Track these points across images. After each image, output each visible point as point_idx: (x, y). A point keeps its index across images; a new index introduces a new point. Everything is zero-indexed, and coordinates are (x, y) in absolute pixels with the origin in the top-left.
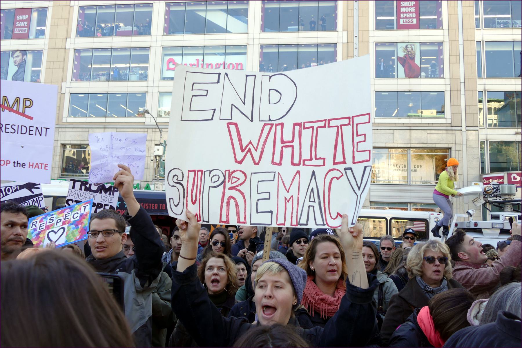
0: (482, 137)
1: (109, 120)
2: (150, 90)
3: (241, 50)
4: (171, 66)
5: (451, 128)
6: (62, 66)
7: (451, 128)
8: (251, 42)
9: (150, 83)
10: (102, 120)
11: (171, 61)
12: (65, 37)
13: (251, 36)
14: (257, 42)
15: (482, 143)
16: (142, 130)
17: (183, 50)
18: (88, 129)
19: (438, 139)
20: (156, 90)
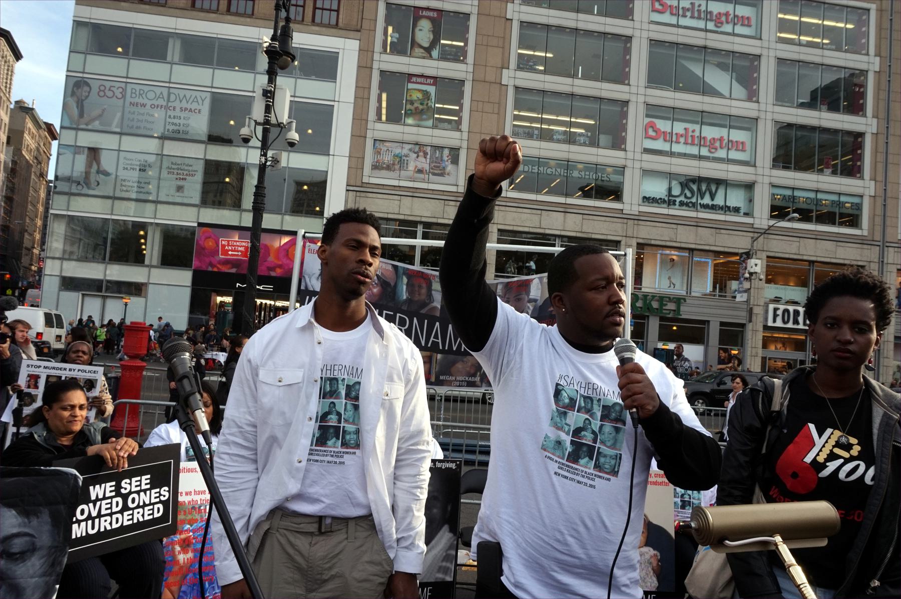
1: (570, 201)
2: (629, 164)
3: (750, 124)
4: (651, 133)
6: (496, 111)
8: (762, 115)
9: (630, 155)
10: (561, 200)
11: (652, 126)
12: (500, 66)
14: (769, 116)
16: (620, 220)
17: (674, 113)
18: (539, 212)
20: (637, 165)
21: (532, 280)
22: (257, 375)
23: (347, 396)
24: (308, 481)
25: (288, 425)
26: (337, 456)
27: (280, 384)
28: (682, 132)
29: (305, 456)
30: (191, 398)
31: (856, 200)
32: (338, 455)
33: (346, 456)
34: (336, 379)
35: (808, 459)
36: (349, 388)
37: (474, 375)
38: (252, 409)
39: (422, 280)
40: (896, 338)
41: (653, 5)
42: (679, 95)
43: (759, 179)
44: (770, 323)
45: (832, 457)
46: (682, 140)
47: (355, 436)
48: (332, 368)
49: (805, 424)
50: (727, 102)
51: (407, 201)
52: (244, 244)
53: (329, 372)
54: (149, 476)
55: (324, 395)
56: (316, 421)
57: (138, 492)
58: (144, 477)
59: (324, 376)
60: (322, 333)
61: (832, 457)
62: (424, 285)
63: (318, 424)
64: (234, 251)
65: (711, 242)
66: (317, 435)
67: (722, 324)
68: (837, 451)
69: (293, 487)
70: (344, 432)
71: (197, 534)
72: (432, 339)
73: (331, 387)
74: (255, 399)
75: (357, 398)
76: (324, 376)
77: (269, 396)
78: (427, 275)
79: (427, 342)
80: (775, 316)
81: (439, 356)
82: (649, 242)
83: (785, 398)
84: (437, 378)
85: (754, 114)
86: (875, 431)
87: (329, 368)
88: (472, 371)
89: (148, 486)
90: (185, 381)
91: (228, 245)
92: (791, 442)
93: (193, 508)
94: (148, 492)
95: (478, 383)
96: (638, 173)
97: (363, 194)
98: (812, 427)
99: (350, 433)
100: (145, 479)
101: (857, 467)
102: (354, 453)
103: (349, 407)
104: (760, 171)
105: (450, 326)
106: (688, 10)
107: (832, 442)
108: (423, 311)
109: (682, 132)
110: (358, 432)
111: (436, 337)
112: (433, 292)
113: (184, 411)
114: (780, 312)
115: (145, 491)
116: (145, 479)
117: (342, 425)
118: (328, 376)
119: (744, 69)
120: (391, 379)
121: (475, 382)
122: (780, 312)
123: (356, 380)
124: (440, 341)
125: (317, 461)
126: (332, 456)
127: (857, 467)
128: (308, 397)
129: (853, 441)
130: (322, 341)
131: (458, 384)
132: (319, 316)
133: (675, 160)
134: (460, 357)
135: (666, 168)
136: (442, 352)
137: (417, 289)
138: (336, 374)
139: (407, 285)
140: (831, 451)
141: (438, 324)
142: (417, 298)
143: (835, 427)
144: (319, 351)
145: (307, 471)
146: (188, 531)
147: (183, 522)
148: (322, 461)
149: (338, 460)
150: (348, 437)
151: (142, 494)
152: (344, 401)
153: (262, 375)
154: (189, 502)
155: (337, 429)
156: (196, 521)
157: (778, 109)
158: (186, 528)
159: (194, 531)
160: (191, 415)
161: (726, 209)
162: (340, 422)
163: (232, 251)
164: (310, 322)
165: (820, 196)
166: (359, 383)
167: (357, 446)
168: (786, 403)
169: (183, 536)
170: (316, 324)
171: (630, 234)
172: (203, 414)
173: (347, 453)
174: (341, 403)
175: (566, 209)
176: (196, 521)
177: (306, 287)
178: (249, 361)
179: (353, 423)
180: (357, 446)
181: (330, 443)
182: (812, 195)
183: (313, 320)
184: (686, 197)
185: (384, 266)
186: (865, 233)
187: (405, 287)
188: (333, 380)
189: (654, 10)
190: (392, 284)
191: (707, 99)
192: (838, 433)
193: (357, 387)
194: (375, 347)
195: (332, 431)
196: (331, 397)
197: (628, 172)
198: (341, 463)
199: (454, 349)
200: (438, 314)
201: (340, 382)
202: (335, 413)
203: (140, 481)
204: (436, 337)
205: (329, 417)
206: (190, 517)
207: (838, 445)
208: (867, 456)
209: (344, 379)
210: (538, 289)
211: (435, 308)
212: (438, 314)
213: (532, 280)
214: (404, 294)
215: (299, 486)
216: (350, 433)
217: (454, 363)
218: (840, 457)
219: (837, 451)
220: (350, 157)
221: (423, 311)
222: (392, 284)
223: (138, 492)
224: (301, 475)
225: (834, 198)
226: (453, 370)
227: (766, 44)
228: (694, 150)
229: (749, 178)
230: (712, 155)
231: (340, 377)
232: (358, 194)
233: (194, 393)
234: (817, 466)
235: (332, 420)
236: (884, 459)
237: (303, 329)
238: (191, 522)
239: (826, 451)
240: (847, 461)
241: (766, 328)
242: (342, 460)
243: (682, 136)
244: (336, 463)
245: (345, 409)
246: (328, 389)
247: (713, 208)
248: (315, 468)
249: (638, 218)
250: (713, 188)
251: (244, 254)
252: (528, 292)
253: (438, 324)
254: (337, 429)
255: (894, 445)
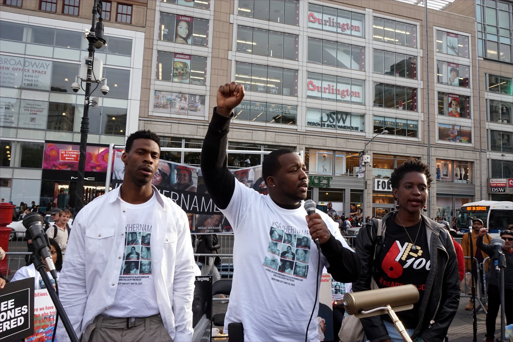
0: (488, 157)
1: (268, 125)
2: (300, 104)
3: (361, 83)
4: (311, 87)
5: (474, 150)
6: (225, 74)
7: (474, 150)
8: (367, 78)
10: (263, 124)
13: (367, 74)
14: (371, 79)
15: (488, 159)
17: (322, 76)
19: (467, 156)
20: (304, 105)
21: (249, 170)
22: (85, 233)
23: (143, 242)
24: (119, 297)
25: (105, 263)
26: (137, 280)
27: (100, 238)
28: (327, 87)
29: (117, 281)
30: (43, 250)
31: (415, 123)
32: (137, 279)
33: (143, 279)
34: (135, 233)
35: (397, 259)
36: (143, 237)
37: (218, 226)
38: (82, 255)
39: (186, 172)
40: (437, 194)
41: (309, 19)
42: (325, 67)
43: (367, 112)
44: (376, 189)
45: (409, 257)
46: (327, 91)
47: (148, 267)
48: (133, 226)
49: (395, 241)
50: (349, 71)
51: (175, 126)
52: (75, 153)
53: (130, 229)
54: (13, 300)
55: (128, 243)
56: (124, 259)
57: (6, 311)
58: (10, 301)
59: (127, 231)
60: (126, 205)
61: (409, 257)
62: (187, 175)
63: (125, 261)
64: (70, 157)
65: (344, 146)
66: (124, 268)
67: (352, 190)
68: (411, 254)
69: (109, 301)
70: (141, 264)
71: (48, 334)
72: (193, 206)
73: (132, 238)
74: (84, 248)
75: (149, 244)
76: (127, 231)
77: (93, 246)
78: (189, 168)
79: (190, 207)
80: (378, 185)
81: (197, 215)
82: (312, 147)
83: (384, 229)
84: (196, 228)
85: (363, 78)
86: (429, 242)
87: (131, 226)
88: (217, 223)
89: (13, 306)
90: (39, 240)
91: (65, 154)
92: (388, 251)
93: (46, 318)
94: (13, 310)
95: (221, 230)
96: (304, 109)
97: (149, 122)
98: (398, 242)
99: (145, 265)
100: (11, 303)
101: (422, 261)
102: (148, 277)
103: (144, 249)
104: (368, 108)
105: (203, 198)
106: (327, 21)
107: (409, 249)
108: (187, 190)
109: (327, 87)
110: (150, 264)
111: (195, 204)
112: (193, 178)
113: (38, 258)
114: (380, 183)
115: (11, 310)
116: (11, 303)
117: (140, 260)
118: (130, 231)
119: (357, 53)
120: (169, 231)
121: (218, 229)
122: (380, 183)
123: (148, 232)
124: (197, 207)
125: (125, 284)
126: (134, 280)
127: (422, 261)
128: (118, 245)
129: (419, 248)
130: (126, 210)
131: (208, 231)
132: (123, 195)
133: (324, 102)
134: (209, 216)
135: (319, 106)
136: (199, 213)
137: (183, 177)
138: (135, 230)
139: (177, 174)
140: (408, 254)
141: (196, 197)
142: (183, 182)
143: (409, 242)
144: (124, 216)
145: (118, 290)
146: (42, 333)
147: (39, 328)
148: (127, 284)
149: (138, 282)
150: (144, 268)
151: (9, 312)
152: (141, 246)
153: (88, 233)
154: (43, 315)
155: (137, 263)
156: (47, 326)
157: (375, 75)
158: (40, 331)
159: (46, 333)
160: (43, 261)
161: (351, 128)
162: (138, 258)
163: (68, 157)
164: (118, 199)
165: (398, 121)
166: (150, 234)
167: (150, 272)
168: (384, 232)
169: (39, 337)
170: (121, 200)
171: (301, 143)
172: (51, 260)
173: (144, 277)
174: (139, 247)
175: (266, 130)
176: (47, 326)
177: (116, 178)
178: (80, 225)
179: (147, 259)
180: (150, 272)
181: (132, 272)
182: (394, 120)
183: (120, 198)
184: (330, 122)
185: (163, 164)
186: (420, 140)
187: (176, 176)
188: (133, 234)
189: (310, 21)
190: (168, 174)
191: (339, 69)
192: (411, 244)
193: (149, 237)
194: (158, 212)
195: (133, 264)
196: (132, 244)
197: (299, 109)
198: (139, 284)
199: (206, 211)
200: (196, 191)
201: (138, 234)
202: (135, 253)
203: (7, 304)
204: (195, 204)
205: (131, 256)
206: (43, 324)
207: (412, 250)
208: (426, 255)
209: (140, 233)
210: (253, 175)
211: (194, 187)
212: (196, 191)
213: (249, 170)
214: (175, 180)
215: (113, 300)
216: (145, 265)
217: (206, 219)
218: (413, 257)
219: (411, 254)
220: (141, 100)
221: (187, 190)
222: (168, 174)
223: (6, 311)
224: (114, 293)
225: (405, 122)
226: (206, 223)
227: (367, 41)
228: (333, 97)
229: (362, 112)
230: (343, 99)
231: (138, 231)
232: (146, 122)
233: (45, 247)
234: (402, 262)
235: (134, 258)
236: (434, 257)
237: (114, 203)
238: (44, 327)
239: (406, 254)
240: (417, 259)
241: (374, 192)
242: (140, 282)
243: (327, 89)
244: (136, 284)
245: (142, 251)
246: (130, 239)
247: (344, 127)
248: (124, 288)
249: (305, 134)
250: (344, 117)
251: (76, 159)
252: (247, 177)
253: (196, 197)
254: (137, 263)
255: (438, 249)
